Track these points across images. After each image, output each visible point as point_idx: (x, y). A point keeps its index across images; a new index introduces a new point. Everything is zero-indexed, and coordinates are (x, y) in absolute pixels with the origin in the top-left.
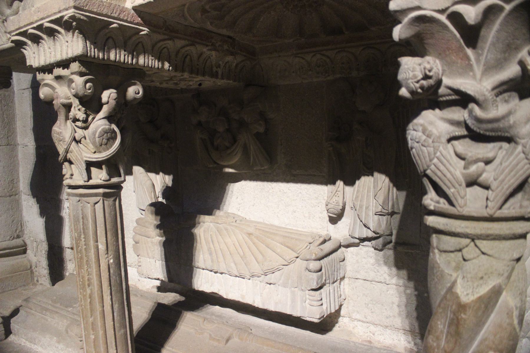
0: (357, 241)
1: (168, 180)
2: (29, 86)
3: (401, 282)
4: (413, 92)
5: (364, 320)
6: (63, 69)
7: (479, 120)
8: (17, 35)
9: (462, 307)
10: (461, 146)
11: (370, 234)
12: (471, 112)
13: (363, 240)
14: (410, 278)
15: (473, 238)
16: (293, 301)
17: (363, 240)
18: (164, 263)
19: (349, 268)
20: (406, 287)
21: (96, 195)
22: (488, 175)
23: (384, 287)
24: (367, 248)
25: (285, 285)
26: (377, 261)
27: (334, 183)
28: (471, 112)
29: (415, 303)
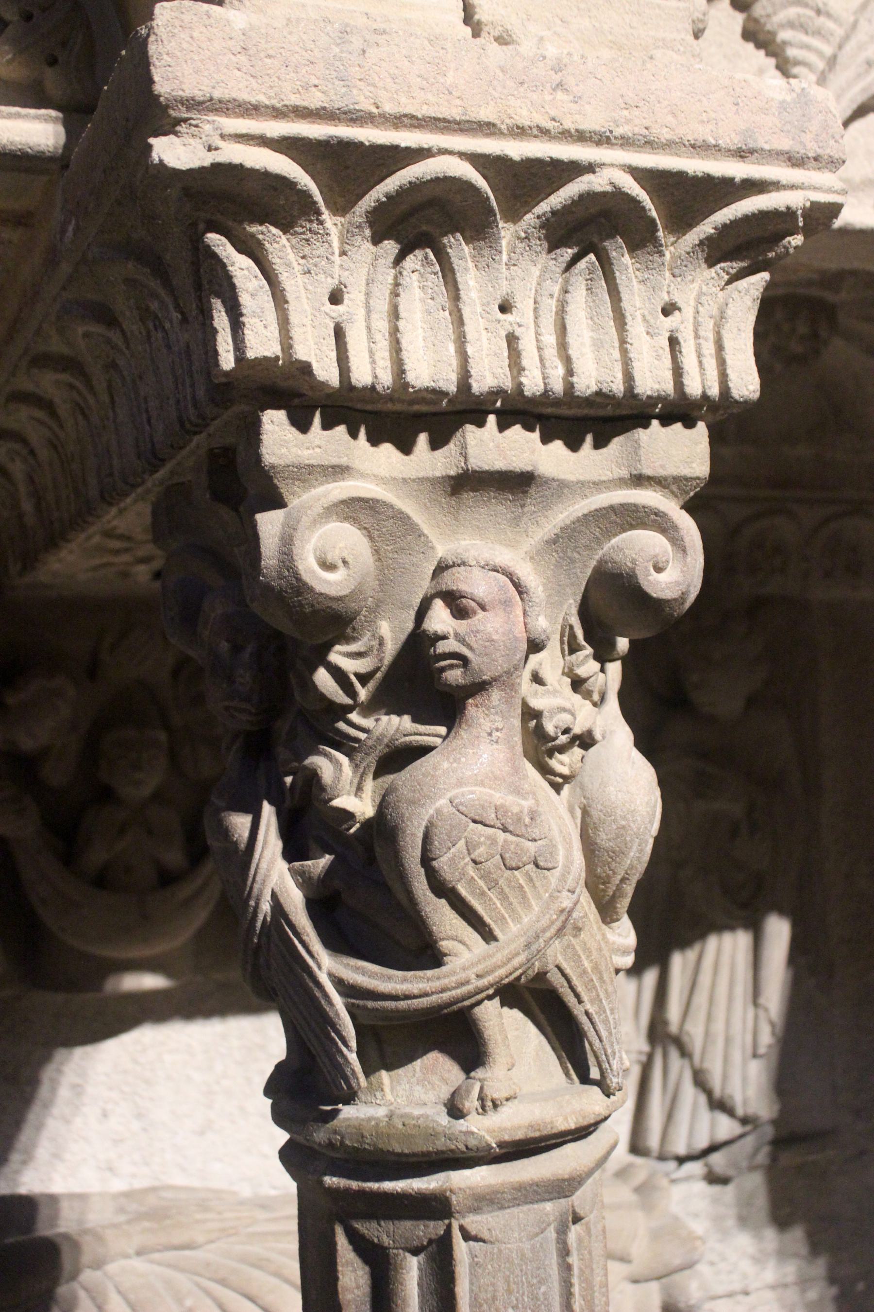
6: (546, 439)
8: (288, 146)
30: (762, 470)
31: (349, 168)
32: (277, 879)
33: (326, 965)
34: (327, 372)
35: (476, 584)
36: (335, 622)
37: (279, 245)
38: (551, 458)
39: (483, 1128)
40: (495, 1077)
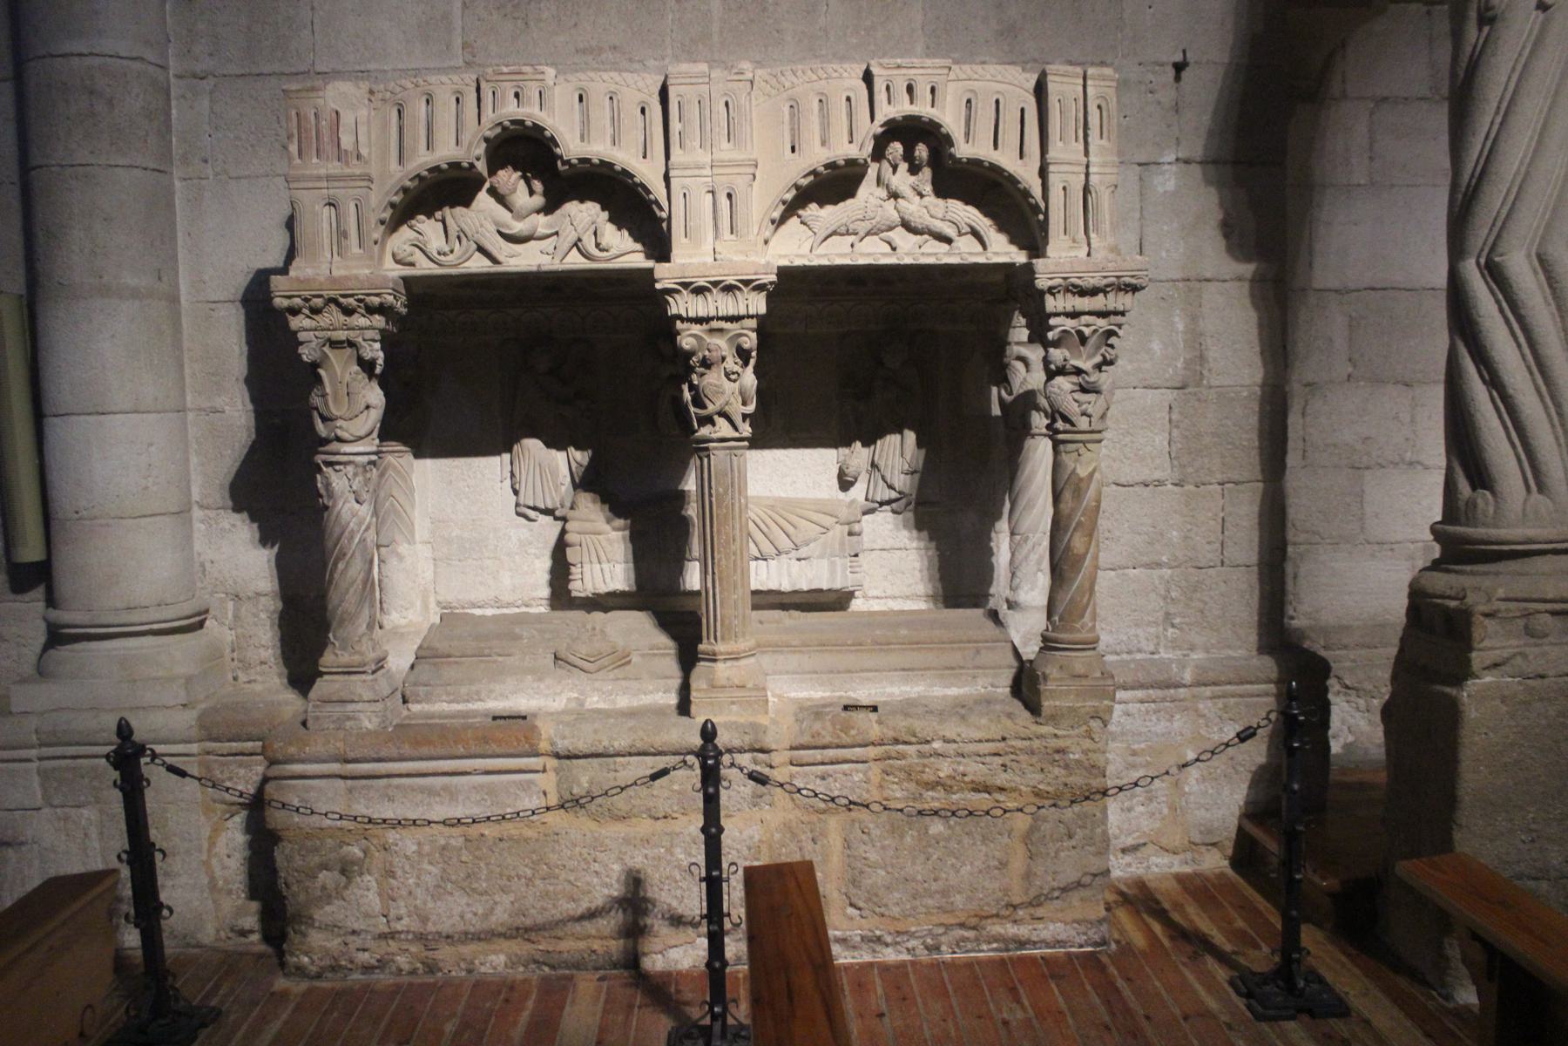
1: (581, 457)
2: (239, 297)
3: (922, 544)
9: (1081, 480)
11: (894, 495)
13: (881, 504)
14: (931, 539)
15: (1083, 442)
16: (833, 572)
17: (881, 504)
18: (631, 565)
20: (927, 549)
22: (1090, 411)
23: (904, 553)
25: (822, 556)
26: (896, 526)
27: (848, 444)
29: (937, 565)
30: (764, 326)
31: (685, 285)
32: (687, 395)
33: (692, 409)
36: (691, 354)
38: (727, 325)
39: (714, 436)
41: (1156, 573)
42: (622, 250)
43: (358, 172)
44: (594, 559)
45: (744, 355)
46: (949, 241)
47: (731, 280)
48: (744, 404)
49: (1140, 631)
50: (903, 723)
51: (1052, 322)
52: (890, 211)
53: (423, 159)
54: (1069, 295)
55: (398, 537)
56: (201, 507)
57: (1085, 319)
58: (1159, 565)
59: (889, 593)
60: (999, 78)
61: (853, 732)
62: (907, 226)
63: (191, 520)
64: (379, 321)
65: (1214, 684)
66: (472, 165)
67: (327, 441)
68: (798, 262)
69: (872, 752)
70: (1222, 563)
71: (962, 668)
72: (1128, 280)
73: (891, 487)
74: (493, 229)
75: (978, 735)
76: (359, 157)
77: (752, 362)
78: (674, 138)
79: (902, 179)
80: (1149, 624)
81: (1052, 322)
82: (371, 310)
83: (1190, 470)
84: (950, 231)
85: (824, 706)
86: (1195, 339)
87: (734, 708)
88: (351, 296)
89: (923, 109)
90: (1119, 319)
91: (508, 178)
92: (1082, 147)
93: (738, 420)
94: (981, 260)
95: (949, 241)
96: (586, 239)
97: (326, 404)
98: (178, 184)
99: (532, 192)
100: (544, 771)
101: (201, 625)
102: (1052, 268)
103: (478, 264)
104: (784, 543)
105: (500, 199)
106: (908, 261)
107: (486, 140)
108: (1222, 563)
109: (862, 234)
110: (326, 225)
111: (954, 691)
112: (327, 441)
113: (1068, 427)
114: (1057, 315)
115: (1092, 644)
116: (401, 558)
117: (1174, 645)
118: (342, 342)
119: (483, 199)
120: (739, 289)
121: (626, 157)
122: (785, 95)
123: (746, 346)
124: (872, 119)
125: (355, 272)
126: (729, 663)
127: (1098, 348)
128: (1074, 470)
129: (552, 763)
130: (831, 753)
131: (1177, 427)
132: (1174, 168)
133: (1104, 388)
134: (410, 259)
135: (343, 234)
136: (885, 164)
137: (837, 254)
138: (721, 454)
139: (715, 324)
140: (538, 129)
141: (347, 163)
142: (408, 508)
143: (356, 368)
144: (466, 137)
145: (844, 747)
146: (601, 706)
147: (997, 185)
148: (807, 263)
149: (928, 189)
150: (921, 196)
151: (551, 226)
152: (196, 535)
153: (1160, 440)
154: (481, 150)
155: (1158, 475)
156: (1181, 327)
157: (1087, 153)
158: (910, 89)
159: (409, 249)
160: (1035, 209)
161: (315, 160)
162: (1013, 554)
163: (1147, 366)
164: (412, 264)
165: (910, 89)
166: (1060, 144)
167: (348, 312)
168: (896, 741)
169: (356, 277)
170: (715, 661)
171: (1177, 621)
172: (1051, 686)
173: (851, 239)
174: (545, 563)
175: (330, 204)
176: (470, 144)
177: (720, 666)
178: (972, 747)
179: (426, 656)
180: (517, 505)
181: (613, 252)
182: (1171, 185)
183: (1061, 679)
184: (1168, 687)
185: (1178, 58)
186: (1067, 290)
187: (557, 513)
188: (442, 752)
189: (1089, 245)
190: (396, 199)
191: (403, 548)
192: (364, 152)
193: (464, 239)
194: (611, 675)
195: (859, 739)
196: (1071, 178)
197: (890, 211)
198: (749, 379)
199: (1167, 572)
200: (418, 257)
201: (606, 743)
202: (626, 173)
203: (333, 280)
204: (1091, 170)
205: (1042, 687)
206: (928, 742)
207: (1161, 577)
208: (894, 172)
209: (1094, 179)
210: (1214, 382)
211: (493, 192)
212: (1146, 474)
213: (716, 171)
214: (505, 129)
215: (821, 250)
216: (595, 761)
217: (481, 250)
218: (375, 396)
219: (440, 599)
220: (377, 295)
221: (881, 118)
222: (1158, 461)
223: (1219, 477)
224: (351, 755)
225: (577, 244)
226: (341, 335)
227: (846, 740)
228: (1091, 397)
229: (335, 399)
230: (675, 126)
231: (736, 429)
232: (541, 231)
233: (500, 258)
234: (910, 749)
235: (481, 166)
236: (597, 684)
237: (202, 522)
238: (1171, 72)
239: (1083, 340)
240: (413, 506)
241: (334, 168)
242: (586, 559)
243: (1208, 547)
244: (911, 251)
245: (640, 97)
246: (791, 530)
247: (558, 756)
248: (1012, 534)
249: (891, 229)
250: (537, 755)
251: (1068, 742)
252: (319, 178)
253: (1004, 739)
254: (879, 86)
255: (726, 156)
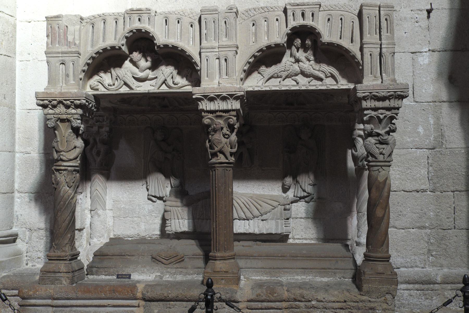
0: (298, 199)
4: (368, 132)
5: (301, 238)
7: (382, 139)
9: (380, 183)
10: (377, 145)
11: (306, 194)
12: (380, 138)
13: (301, 198)
15: (381, 166)
16: (277, 226)
19: (293, 213)
21: (230, 167)
22: (384, 152)
24: (302, 203)
25: (272, 219)
28: (380, 138)
31: (206, 97)
32: (208, 145)
34: (205, 109)
35: (217, 123)
37: (202, 102)
38: (224, 114)
39: (217, 161)
40: (219, 158)
41: (424, 231)
42: (182, 84)
43: (74, 50)
44: (176, 217)
45: (231, 127)
46: (321, 79)
47: (224, 94)
48: (231, 148)
49: (416, 257)
50: (298, 292)
51: (365, 112)
52: (296, 67)
53: (101, 45)
54: (373, 101)
55: (98, 207)
56: (19, 192)
57: (380, 111)
58: (424, 228)
59: (304, 237)
60: (342, 9)
61: (275, 295)
62: (303, 73)
63: (13, 198)
64: (80, 111)
65: (452, 283)
66: (120, 48)
67: (57, 160)
68: (256, 89)
69: (284, 304)
70: (455, 227)
71: (329, 269)
72: (399, 93)
73: (304, 191)
74: (131, 75)
75: (333, 299)
76: (75, 44)
77: (236, 130)
78: (203, 36)
79: (301, 54)
80: (420, 254)
81: (365, 112)
82: (77, 107)
83: (438, 185)
84: (322, 76)
85: (264, 283)
86: (439, 127)
87: (223, 281)
88: (68, 100)
89: (309, 22)
90: (396, 111)
91: (136, 55)
92: (378, 37)
93: (228, 155)
94: (336, 87)
95: (321, 79)
96: (166, 80)
97: (58, 145)
98: (18, 63)
99: (147, 61)
100: (139, 306)
101: (14, 241)
102: (364, 88)
103: (124, 90)
104: (256, 213)
105: (134, 63)
106: (304, 88)
107: (126, 38)
108: (455, 227)
109: (284, 77)
110: (61, 72)
111: (325, 280)
112: (57, 160)
113: (374, 159)
114: (367, 109)
115: (387, 259)
116: (99, 216)
117: (433, 265)
118: (65, 119)
119: (127, 63)
120: (229, 99)
121: (182, 44)
122: (251, 19)
123: (231, 123)
124: (287, 27)
125: (71, 91)
126: (222, 262)
127: (387, 124)
128: (376, 179)
129: (142, 303)
130: (265, 304)
131: (431, 166)
132: (428, 54)
133: (391, 142)
134: (97, 87)
135: (67, 75)
136: (293, 48)
137: (274, 85)
138: (220, 169)
139: (218, 114)
140: (147, 33)
141: (70, 47)
142: (103, 195)
143: (71, 130)
144: (118, 37)
145: (271, 302)
146: (170, 279)
147: (343, 55)
148: (260, 89)
149: (312, 58)
150: (309, 60)
151: (154, 75)
152: (16, 204)
153: (424, 172)
154: (124, 41)
155: (423, 187)
156: (432, 122)
157: (380, 39)
158: (303, 15)
159: (96, 83)
160: (358, 63)
161: (57, 46)
162: (358, 221)
163: (417, 139)
164: (97, 90)
165: (303, 15)
166: (368, 36)
167: (67, 107)
168: (295, 300)
169: (70, 93)
170: (216, 260)
171: (434, 253)
172: (367, 277)
173: (279, 79)
174: (158, 221)
175: (63, 64)
176: (119, 39)
177: (218, 262)
178: (330, 305)
179: (100, 255)
180: (148, 195)
181: (180, 85)
182: (426, 61)
183: (372, 274)
184: (430, 284)
185: (429, 7)
186: (372, 98)
187: (164, 199)
188: (95, 296)
189: (382, 79)
190: (90, 62)
191: (100, 212)
192: (77, 42)
193: (119, 79)
194: (175, 266)
195: (278, 298)
196: (373, 50)
197: (296, 67)
198: (234, 137)
199: (428, 231)
200: (100, 87)
201: (166, 295)
202: (183, 51)
203: (61, 93)
204: (383, 46)
205: (363, 278)
206: (310, 301)
207: (426, 233)
208: (298, 51)
209: (384, 50)
210: (448, 146)
211: (132, 61)
212: (417, 187)
213: (220, 49)
214: (134, 33)
215: (267, 84)
216: (161, 303)
217: (126, 84)
218: (79, 143)
219: (115, 233)
220: (79, 100)
221: (290, 26)
222: (423, 181)
223: (452, 189)
224: (56, 296)
225: (164, 82)
226: (64, 117)
227: (272, 298)
228: (384, 146)
229: (61, 143)
230: (204, 31)
231: (227, 158)
232: (151, 76)
233: (133, 87)
234: (302, 304)
235: (124, 48)
236: (169, 270)
237: (19, 198)
238: (426, 13)
239: (380, 121)
240: (106, 195)
241: (65, 49)
242: (172, 217)
243: (448, 220)
244: (304, 84)
245: (191, 20)
246: (259, 207)
247: (144, 299)
248: (358, 212)
249: (296, 75)
250: (136, 299)
251: (376, 305)
252: (58, 53)
253: (345, 301)
254: (290, 13)
255: (224, 43)
